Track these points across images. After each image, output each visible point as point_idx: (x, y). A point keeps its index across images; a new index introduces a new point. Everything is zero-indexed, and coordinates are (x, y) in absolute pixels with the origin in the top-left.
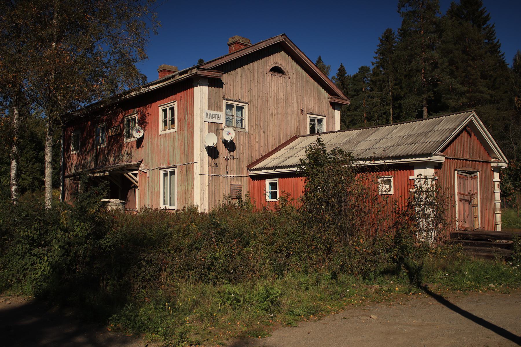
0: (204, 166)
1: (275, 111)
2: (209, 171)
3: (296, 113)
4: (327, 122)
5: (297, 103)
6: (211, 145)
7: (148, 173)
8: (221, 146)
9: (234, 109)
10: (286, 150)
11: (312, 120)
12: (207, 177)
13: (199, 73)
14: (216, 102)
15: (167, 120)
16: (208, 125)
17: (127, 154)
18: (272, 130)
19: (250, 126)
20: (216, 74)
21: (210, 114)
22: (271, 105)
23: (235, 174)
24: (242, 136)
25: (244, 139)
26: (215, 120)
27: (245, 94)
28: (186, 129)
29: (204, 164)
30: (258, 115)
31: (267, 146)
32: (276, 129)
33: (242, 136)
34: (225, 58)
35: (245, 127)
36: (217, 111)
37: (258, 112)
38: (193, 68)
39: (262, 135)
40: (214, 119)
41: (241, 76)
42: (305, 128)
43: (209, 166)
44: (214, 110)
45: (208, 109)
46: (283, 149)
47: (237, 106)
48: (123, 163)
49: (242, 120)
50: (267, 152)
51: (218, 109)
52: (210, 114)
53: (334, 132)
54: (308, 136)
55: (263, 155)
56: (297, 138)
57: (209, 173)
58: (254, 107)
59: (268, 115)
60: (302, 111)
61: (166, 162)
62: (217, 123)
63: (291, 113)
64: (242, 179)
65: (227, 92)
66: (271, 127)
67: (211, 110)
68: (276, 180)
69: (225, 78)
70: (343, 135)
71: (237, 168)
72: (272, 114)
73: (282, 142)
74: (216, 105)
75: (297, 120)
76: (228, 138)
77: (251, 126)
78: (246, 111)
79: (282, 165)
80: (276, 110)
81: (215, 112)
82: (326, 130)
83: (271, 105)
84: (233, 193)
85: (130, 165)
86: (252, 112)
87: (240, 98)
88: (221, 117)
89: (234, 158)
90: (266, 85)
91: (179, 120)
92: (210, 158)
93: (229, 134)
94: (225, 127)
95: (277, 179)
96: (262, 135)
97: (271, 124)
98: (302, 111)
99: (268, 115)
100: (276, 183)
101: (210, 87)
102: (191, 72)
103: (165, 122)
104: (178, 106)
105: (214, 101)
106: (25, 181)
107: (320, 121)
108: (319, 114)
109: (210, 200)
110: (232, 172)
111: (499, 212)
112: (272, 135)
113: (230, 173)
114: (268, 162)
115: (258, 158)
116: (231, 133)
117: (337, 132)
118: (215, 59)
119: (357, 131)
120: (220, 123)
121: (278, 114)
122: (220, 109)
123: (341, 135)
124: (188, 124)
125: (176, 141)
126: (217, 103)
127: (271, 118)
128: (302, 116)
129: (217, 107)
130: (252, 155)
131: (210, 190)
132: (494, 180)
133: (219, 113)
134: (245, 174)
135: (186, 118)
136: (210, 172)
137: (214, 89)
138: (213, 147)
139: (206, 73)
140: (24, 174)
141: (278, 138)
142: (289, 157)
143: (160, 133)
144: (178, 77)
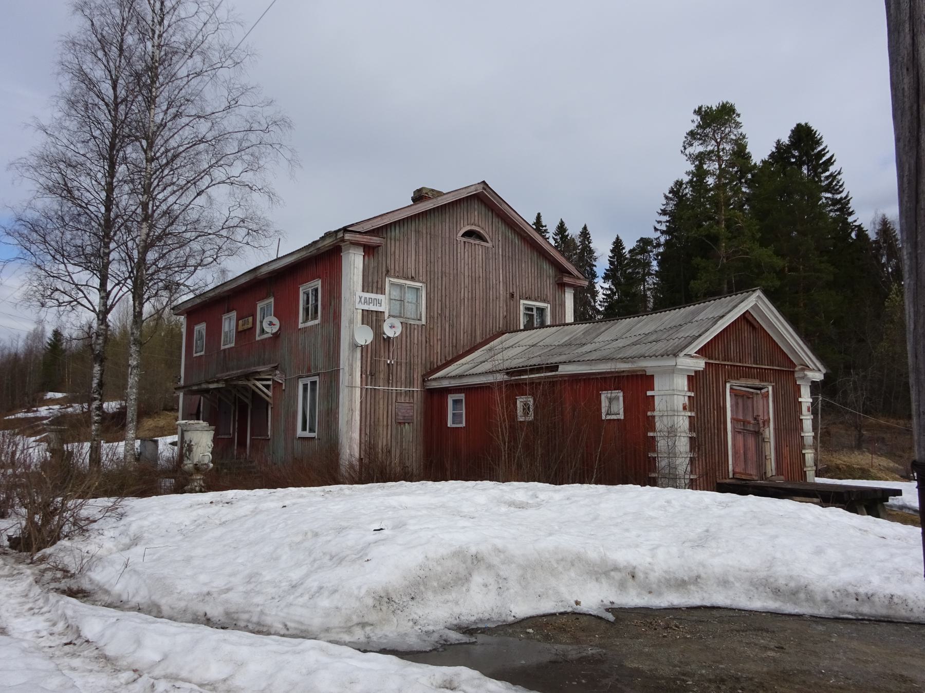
0: (354, 374)
2: (361, 382)
5: (505, 283)
7: (284, 384)
10: (483, 352)
14: (375, 281)
15: (309, 308)
16: (363, 315)
18: (464, 321)
19: (428, 316)
20: (375, 240)
21: (366, 298)
23: (403, 386)
24: (416, 332)
25: (419, 335)
26: (372, 308)
27: (422, 271)
28: (332, 319)
29: (354, 372)
30: (441, 301)
31: (456, 346)
33: (416, 332)
35: (421, 317)
36: (377, 293)
37: (442, 296)
39: (447, 330)
40: (371, 305)
41: (417, 243)
43: (361, 375)
44: (372, 293)
45: (363, 291)
46: (479, 351)
50: (455, 355)
52: (366, 298)
54: (521, 330)
55: (449, 359)
56: (503, 334)
57: (361, 385)
58: (436, 289)
59: (458, 301)
60: (512, 295)
62: (376, 311)
63: (495, 299)
64: (415, 394)
65: (393, 267)
66: (462, 317)
67: (368, 292)
68: (462, 396)
70: (564, 332)
71: (406, 377)
72: (464, 299)
73: (479, 340)
74: (375, 285)
77: (430, 317)
79: (471, 372)
81: (373, 296)
84: (400, 414)
86: (432, 295)
87: (413, 275)
90: (455, 258)
93: (392, 327)
94: (388, 318)
95: (463, 395)
96: (447, 330)
97: (462, 313)
99: (458, 301)
100: (462, 400)
102: (336, 236)
103: (306, 310)
104: (322, 287)
105: (373, 280)
109: (363, 424)
110: (399, 384)
111: (811, 452)
112: (464, 329)
113: (396, 384)
114: (452, 370)
115: (439, 363)
116: (396, 325)
119: (584, 326)
120: (381, 312)
121: (473, 299)
123: (562, 330)
124: (335, 313)
126: (377, 282)
127: (462, 305)
128: (511, 301)
129: (377, 288)
130: (432, 359)
131: (364, 409)
132: (800, 400)
133: (379, 297)
134: (419, 386)
135: (333, 303)
136: (364, 383)
139: (358, 238)
141: (474, 335)
142: (481, 363)
144: (320, 245)
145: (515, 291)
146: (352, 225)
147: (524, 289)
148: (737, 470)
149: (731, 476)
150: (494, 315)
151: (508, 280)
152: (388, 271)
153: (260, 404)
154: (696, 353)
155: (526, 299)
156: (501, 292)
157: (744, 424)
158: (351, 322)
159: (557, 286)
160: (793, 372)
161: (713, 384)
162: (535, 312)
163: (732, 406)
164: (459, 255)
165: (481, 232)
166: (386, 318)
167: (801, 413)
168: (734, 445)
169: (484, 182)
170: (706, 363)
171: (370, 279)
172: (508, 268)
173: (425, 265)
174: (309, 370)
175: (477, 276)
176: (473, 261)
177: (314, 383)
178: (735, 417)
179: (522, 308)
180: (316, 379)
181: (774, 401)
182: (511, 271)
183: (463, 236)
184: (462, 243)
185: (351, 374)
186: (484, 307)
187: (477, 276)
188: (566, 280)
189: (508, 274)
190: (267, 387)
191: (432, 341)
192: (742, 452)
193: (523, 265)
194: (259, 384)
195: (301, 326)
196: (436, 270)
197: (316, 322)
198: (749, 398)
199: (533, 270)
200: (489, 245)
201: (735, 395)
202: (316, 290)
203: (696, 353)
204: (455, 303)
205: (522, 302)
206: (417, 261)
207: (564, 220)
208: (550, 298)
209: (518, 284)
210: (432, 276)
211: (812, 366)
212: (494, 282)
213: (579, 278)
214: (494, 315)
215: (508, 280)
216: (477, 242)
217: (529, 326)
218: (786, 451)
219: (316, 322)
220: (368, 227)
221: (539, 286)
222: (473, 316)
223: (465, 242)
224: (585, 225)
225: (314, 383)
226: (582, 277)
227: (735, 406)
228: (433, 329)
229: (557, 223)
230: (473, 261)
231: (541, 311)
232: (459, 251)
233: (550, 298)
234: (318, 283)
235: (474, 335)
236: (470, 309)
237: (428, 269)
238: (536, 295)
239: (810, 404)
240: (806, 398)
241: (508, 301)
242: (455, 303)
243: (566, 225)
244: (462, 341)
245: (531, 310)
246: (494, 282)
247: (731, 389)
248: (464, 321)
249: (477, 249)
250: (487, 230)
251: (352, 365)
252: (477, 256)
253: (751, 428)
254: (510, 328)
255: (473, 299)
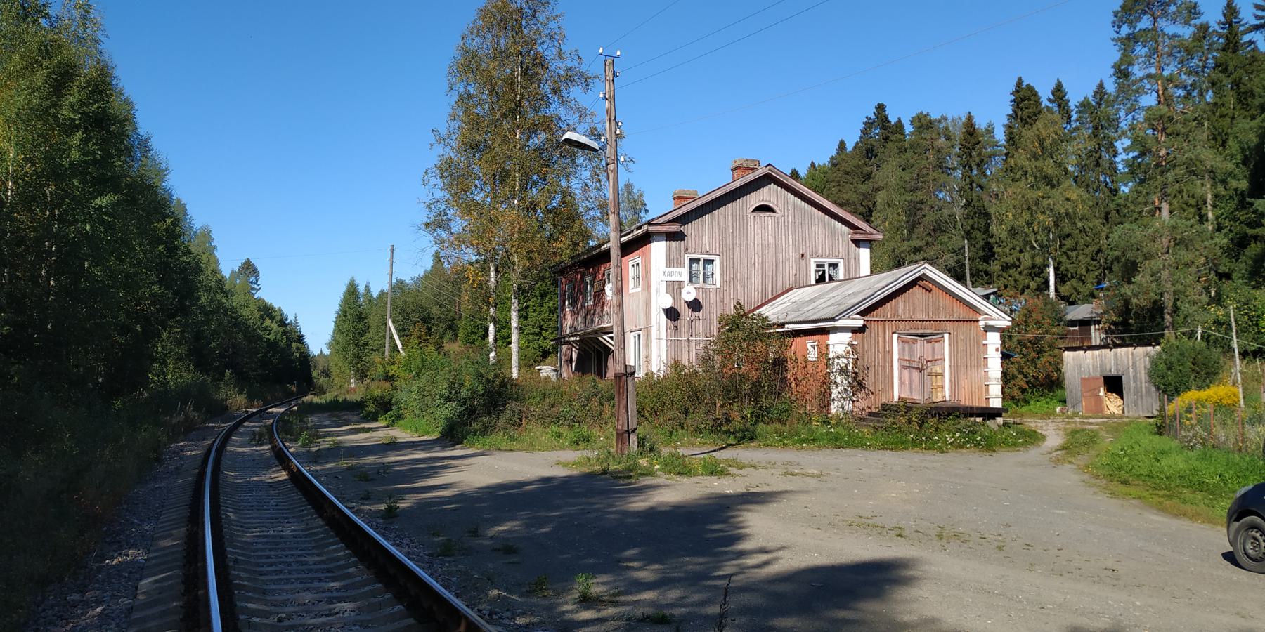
1: (758, 260)
2: (667, 335)
3: (792, 259)
4: (845, 266)
6: (668, 307)
8: (683, 307)
9: (702, 262)
11: (818, 266)
12: (664, 343)
13: (651, 229)
16: (666, 285)
17: (608, 314)
18: (755, 281)
19: (722, 281)
20: (674, 228)
22: (753, 253)
27: (716, 245)
32: (760, 281)
34: (684, 207)
38: (645, 224)
42: (808, 276)
47: (704, 260)
48: (596, 326)
49: (713, 274)
51: (679, 266)
53: (860, 277)
60: (803, 255)
61: (634, 325)
63: (784, 260)
65: (690, 245)
69: (688, 229)
72: (754, 264)
73: (770, 297)
75: (794, 268)
76: (691, 298)
77: (724, 281)
78: (717, 263)
80: (760, 259)
81: (675, 269)
82: (845, 275)
83: (753, 253)
85: (605, 328)
86: (725, 264)
88: (683, 274)
89: (699, 319)
91: (642, 279)
92: (669, 320)
93: (688, 293)
98: (803, 255)
101: (668, 242)
106: (547, 341)
107: (835, 266)
108: (831, 256)
117: (841, 281)
118: (669, 211)
121: (764, 262)
122: (682, 265)
124: (648, 283)
125: (641, 301)
133: (679, 270)
137: (674, 244)
138: (671, 308)
140: (546, 331)
141: (764, 292)
143: (631, 291)
144: (637, 232)
145: (804, 251)
146: (654, 219)
147: (814, 249)
148: (903, 396)
149: (896, 399)
150: (784, 273)
151: (797, 242)
152: (687, 249)
153: (608, 351)
154: (858, 314)
155: (818, 257)
156: (791, 254)
157: (909, 363)
158: (658, 291)
159: (850, 242)
160: (977, 321)
161: (878, 334)
162: (826, 268)
163: (899, 350)
164: (749, 227)
165: (771, 205)
166: (686, 285)
167: (986, 352)
168: (900, 378)
169: (769, 165)
170: (865, 320)
171: (671, 257)
172: (797, 234)
173: (717, 241)
174: (636, 327)
175: (767, 243)
176: (763, 231)
177: (639, 335)
178: (902, 357)
179: (813, 267)
180: (640, 333)
181: (950, 345)
182: (800, 234)
183: (753, 211)
184: (752, 216)
185: (659, 330)
186: (774, 267)
187: (767, 241)
188: (858, 237)
189: (797, 238)
190: (611, 338)
191: (725, 300)
192: (907, 383)
193: (813, 228)
194: (605, 337)
195: (631, 291)
196: (728, 243)
197: (639, 289)
198: (914, 343)
199: (824, 232)
200: (779, 214)
201: (902, 342)
202: (638, 264)
203: (858, 314)
204: (746, 268)
205: (812, 260)
206: (711, 237)
207: (1061, 80)
208: (842, 253)
209: (808, 245)
210: (725, 249)
211: (995, 316)
212: (784, 245)
213: (872, 234)
214: (784, 273)
215: (797, 242)
216: (768, 214)
217: (821, 280)
218: (965, 383)
219: (639, 289)
220: (668, 217)
221: (831, 244)
222: (764, 277)
223: (755, 216)
224: (1101, 81)
225: (639, 335)
226: (875, 232)
227: (902, 351)
228: (726, 290)
229: (1052, 85)
230: (763, 231)
231: (835, 266)
232: (749, 224)
233: (842, 253)
234: (639, 260)
235: (764, 292)
236: (760, 271)
237: (721, 243)
238: (827, 253)
239: (999, 346)
240: (994, 340)
241: (798, 260)
242: (746, 268)
243: (1064, 86)
244: (753, 298)
245: (823, 266)
246: (784, 245)
247: (899, 337)
248: (755, 281)
249: (768, 220)
250: (776, 203)
251: (659, 323)
252: (766, 226)
253: (915, 365)
254: (798, 285)
255: (764, 262)
